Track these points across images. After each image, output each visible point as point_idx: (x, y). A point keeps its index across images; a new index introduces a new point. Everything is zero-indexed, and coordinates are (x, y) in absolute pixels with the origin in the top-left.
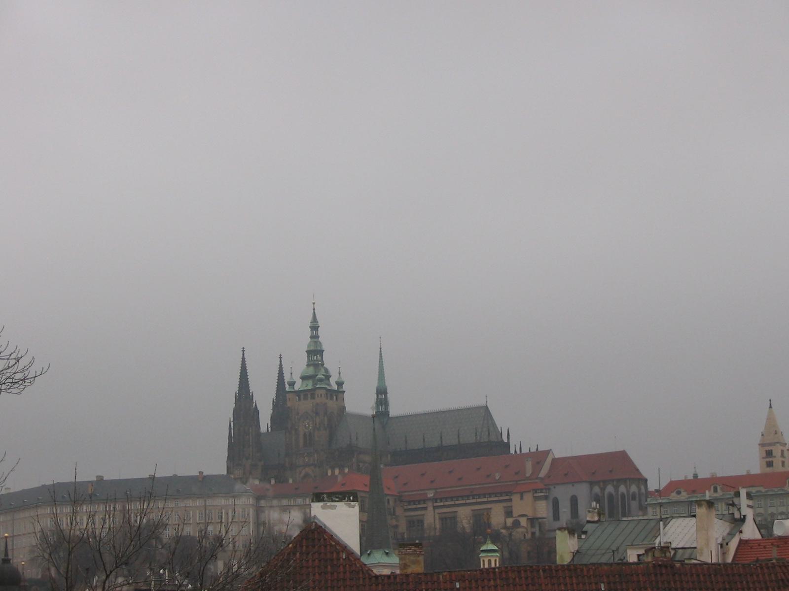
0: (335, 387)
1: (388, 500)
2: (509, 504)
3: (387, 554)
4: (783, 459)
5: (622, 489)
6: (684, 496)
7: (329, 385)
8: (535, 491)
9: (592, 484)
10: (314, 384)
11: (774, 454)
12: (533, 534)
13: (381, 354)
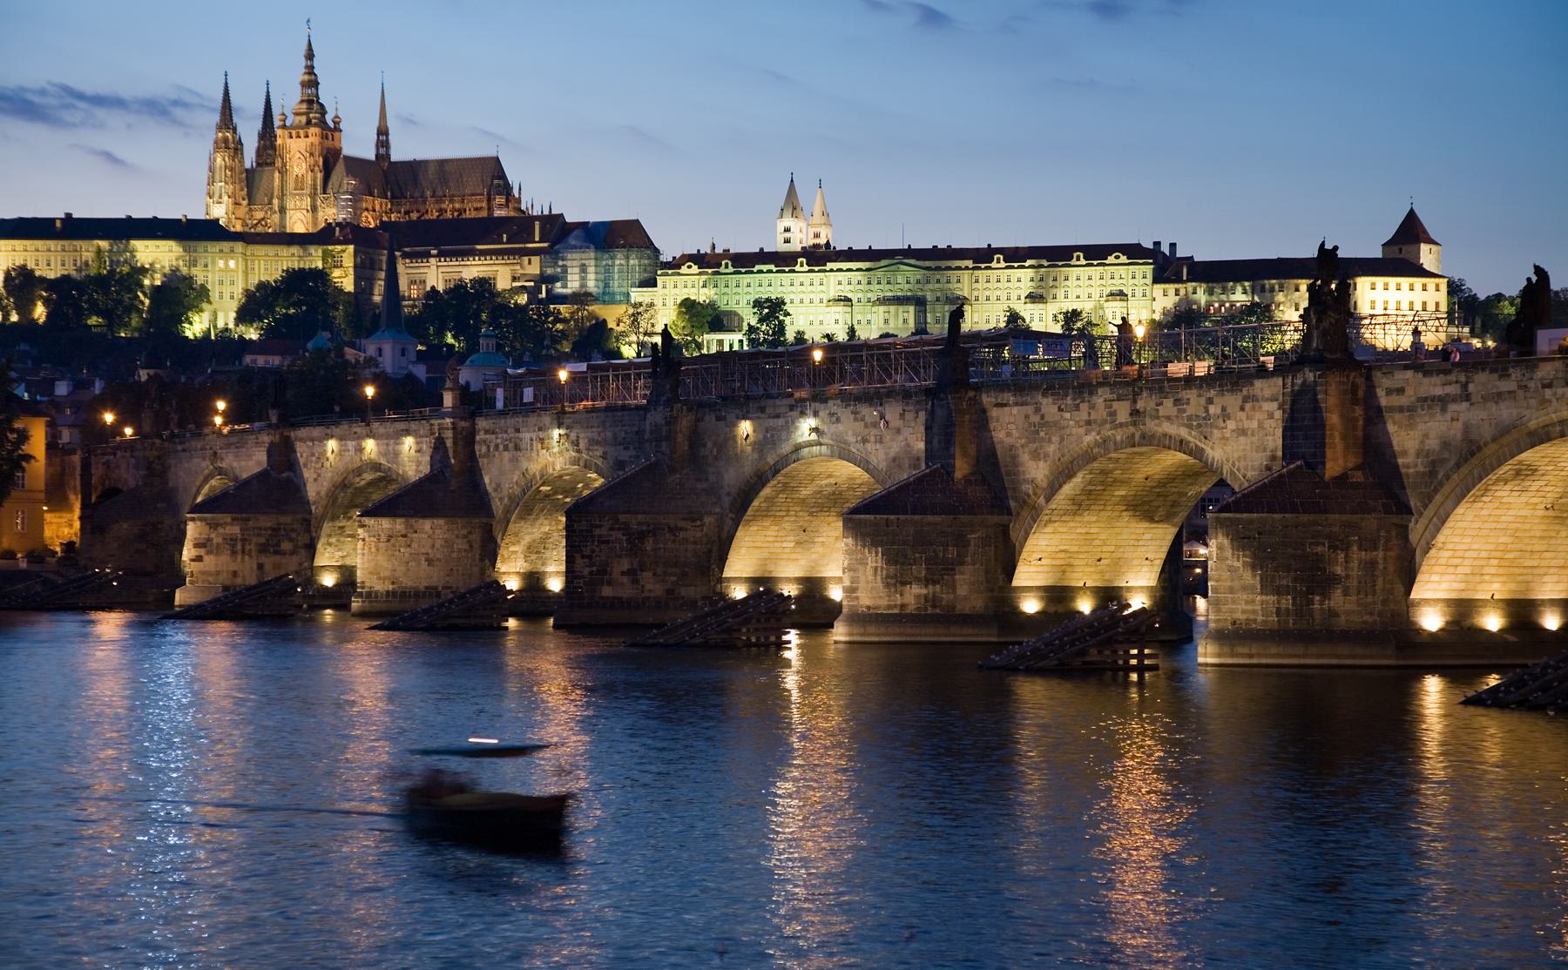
0: (332, 125)
10: (309, 123)
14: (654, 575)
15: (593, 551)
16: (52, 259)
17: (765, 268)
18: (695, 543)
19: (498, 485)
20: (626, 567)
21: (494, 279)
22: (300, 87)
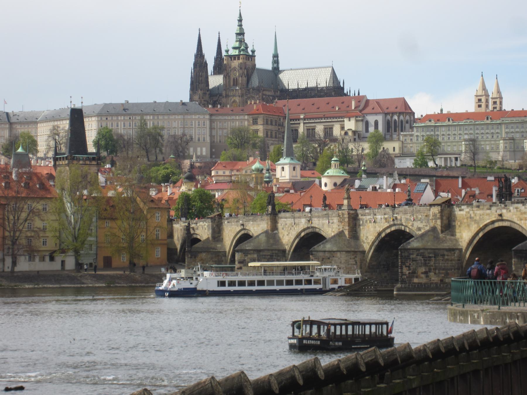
0: (251, 53)
1: (280, 119)
2: (343, 123)
3: (292, 159)
4: (487, 104)
5: (402, 117)
6: (433, 123)
7: (247, 52)
8: (357, 117)
9: (386, 114)
10: (240, 51)
11: (482, 101)
12: (355, 140)
13: (276, 35)
14: (435, 274)
15: (410, 264)
16: (119, 123)
17: (468, 121)
18: (451, 261)
19: (367, 237)
20: (423, 269)
21: (332, 128)
22: (235, 35)
